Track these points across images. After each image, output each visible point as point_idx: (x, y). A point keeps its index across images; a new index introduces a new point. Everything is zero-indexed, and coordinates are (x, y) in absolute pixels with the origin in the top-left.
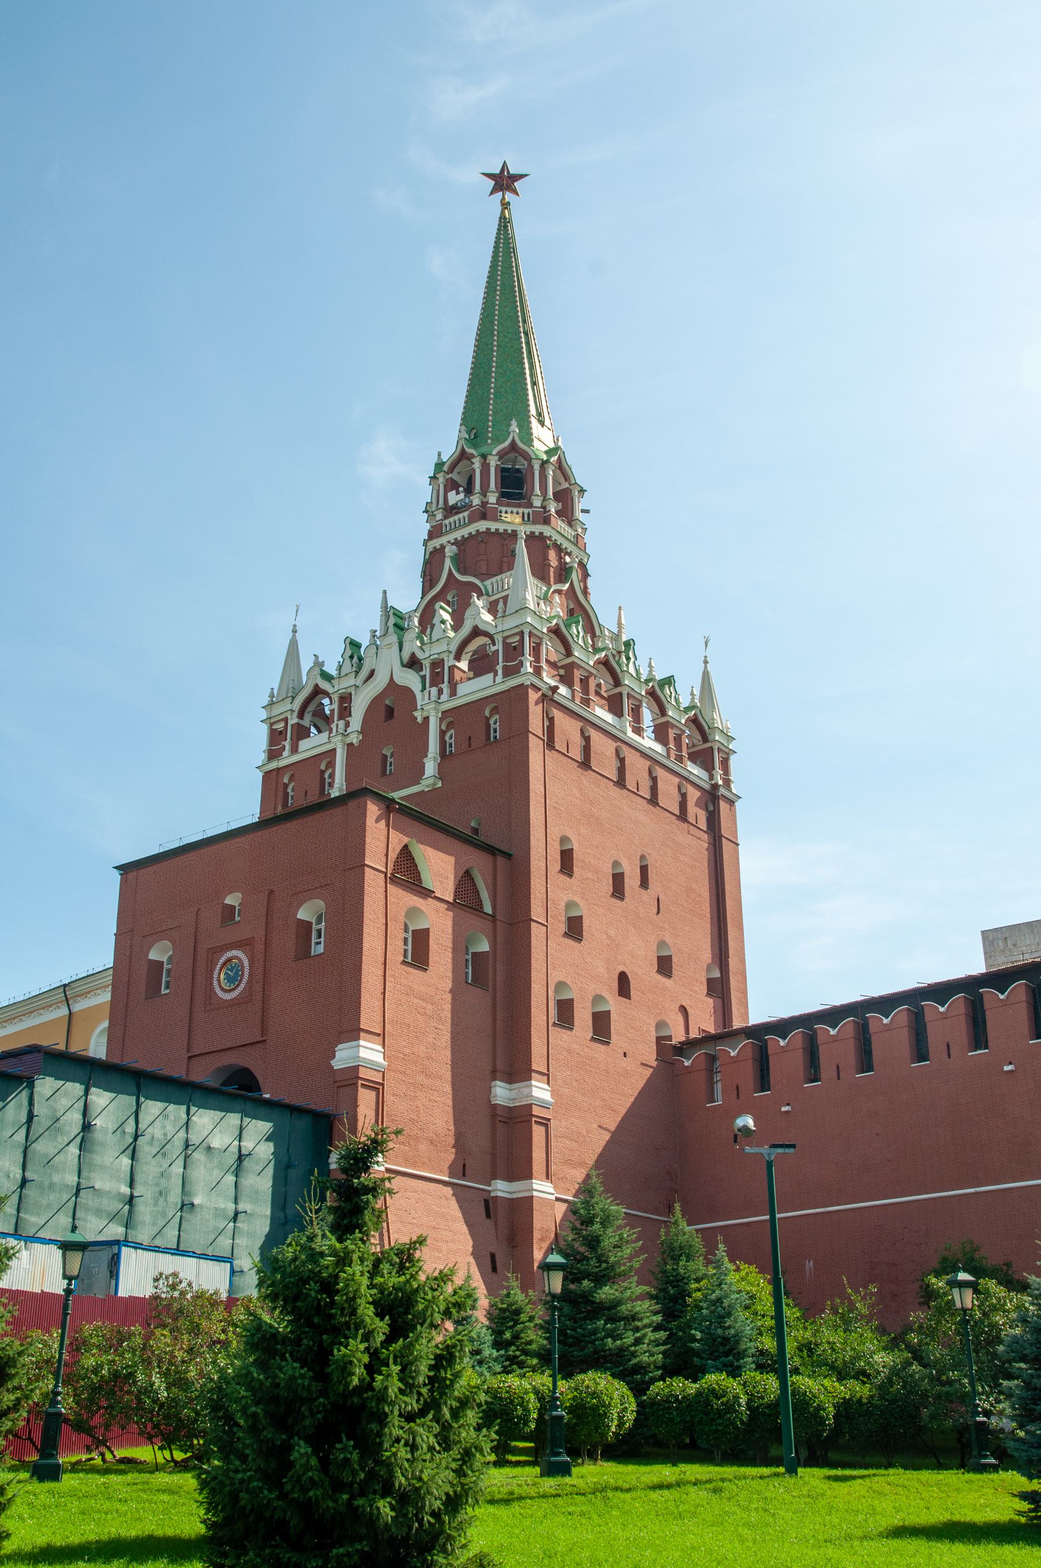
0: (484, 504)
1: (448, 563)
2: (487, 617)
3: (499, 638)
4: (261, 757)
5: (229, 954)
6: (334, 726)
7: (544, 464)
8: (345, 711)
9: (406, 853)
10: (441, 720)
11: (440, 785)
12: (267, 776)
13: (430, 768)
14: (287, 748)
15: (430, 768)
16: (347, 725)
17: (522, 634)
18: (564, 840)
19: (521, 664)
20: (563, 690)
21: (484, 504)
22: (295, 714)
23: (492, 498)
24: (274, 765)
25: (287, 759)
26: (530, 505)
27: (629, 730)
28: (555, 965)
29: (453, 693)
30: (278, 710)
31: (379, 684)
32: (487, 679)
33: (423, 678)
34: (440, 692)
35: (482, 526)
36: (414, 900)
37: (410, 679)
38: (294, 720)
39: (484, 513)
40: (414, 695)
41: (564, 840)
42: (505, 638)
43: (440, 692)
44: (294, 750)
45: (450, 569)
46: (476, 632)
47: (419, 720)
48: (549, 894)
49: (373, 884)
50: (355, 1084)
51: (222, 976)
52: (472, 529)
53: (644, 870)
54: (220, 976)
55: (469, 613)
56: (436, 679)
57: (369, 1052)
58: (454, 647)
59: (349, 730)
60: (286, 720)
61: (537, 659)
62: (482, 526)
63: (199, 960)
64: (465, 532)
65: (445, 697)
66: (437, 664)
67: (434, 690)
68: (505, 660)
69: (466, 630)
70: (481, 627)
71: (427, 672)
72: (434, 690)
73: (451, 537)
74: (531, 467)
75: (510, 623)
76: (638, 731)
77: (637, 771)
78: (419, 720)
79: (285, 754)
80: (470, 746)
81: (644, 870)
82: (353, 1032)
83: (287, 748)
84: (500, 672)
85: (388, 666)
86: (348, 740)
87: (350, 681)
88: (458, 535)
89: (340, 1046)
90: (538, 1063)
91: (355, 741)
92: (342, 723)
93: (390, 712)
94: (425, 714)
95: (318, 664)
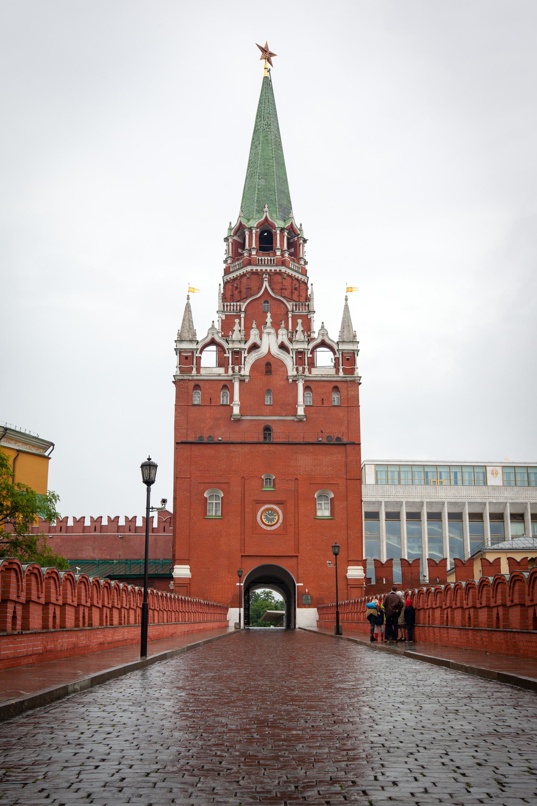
0: (282, 255)
1: (266, 284)
5: (268, 506)
6: (230, 366)
10: (303, 384)
11: (305, 420)
14: (194, 369)
16: (240, 369)
21: (282, 255)
22: (198, 352)
23: (286, 255)
26: (299, 263)
29: (310, 373)
30: (185, 346)
34: (304, 369)
35: (283, 269)
38: (198, 355)
39: (283, 263)
40: (284, 366)
43: (304, 369)
45: (266, 288)
47: (291, 380)
51: (263, 517)
52: (278, 269)
59: (242, 373)
62: (283, 269)
64: (273, 269)
65: (307, 373)
66: (300, 353)
70: (327, 341)
71: (293, 354)
72: (301, 368)
73: (264, 269)
78: (291, 380)
79: (194, 372)
80: (323, 404)
83: (194, 369)
84: (341, 370)
86: (242, 378)
87: (242, 346)
88: (268, 269)
89: (349, 567)
91: (247, 380)
92: (237, 368)
94: (295, 379)
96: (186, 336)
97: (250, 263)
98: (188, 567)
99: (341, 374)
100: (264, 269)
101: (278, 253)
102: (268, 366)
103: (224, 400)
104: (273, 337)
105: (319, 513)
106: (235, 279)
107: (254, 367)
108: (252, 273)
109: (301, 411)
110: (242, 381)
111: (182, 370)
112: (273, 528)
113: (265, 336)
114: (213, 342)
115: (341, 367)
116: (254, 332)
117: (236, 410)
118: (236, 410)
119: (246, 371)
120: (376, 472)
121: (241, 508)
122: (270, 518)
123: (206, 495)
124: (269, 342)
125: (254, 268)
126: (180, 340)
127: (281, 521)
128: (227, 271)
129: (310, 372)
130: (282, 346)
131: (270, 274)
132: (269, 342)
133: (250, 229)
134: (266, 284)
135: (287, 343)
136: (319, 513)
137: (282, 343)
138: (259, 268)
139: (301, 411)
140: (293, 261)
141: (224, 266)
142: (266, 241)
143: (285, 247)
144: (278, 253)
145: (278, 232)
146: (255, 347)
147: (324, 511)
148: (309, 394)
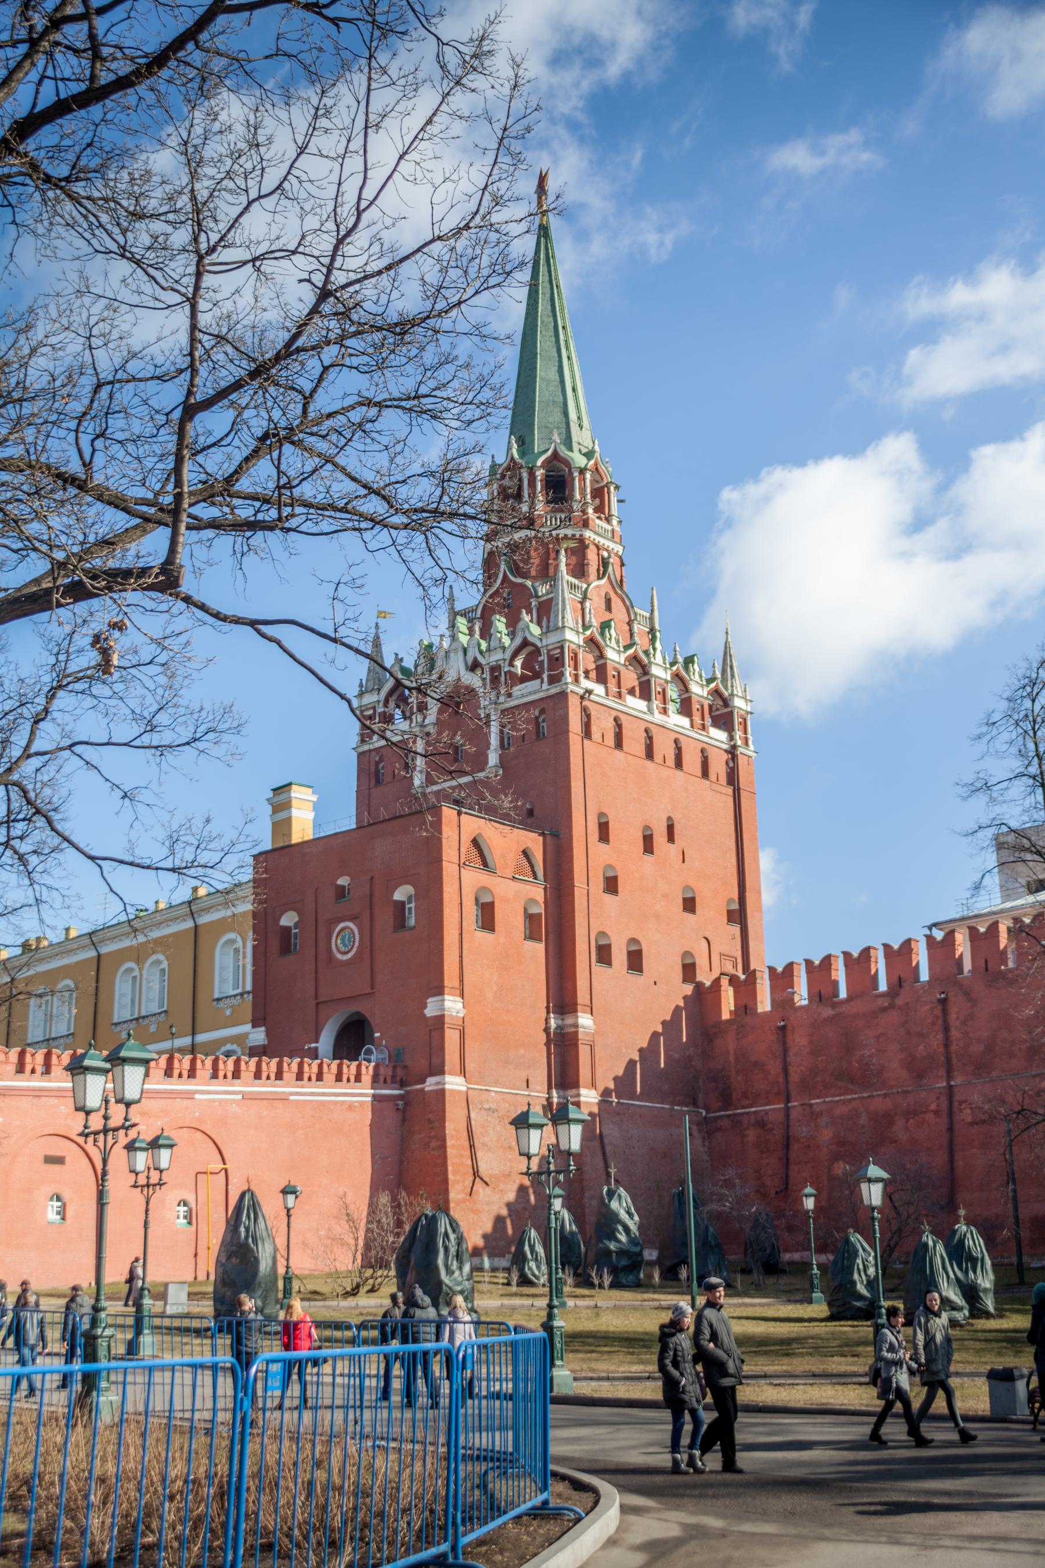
2: (535, 630)
3: (544, 651)
5: (342, 925)
7: (582, 471)
8: (422, 707)
9: (475, 843)
12: (361, 755)
13: (493, 758)
15: (493, 758)
17: (562, 648)
18: (601, 815)
19: (562, 674)
20: (599, 689)
24: (366, 748)
27: (656, 712)
28: (596, 915)
32: (534, 684)
33: (484, 679)
36: (482, 878)
37: (473, 680)
41: (601, 815)
42: (549, 651)
43: (498, 695)
46: (525, 643)
48: (589, 859)
49: (449, 869)
50: (443, 1028)
53: (670, 828)
54: (336, 942)
55: (521, 625)
56: (495, 680)
57: (452, 1005)
58: (508, 655)
59: (427, 722)
60: (374, 708)
61: (576, 668)
63: (319, 927)
65: (502, 699)
66: (495, 669)
67: (494, 693)
68: (549, 670)
69: (518, 641)
70: (530, 639)
71: (487, 675)
74: (571, 473)
75: (552, 639)
76: (665, 711)
77: (664, 748)
81: (670, 828)
82: (439, 990)
85: (456, 670)
86: (427, 730)
90: (582, 997)
95: (399, 660)
98: (263, 1029)
99: (545, 686)
112: (349, 956)
115: (545, 676)
127: (357, 944)
134: (503, 567)
137: (475, 659)
145: (525, 475)
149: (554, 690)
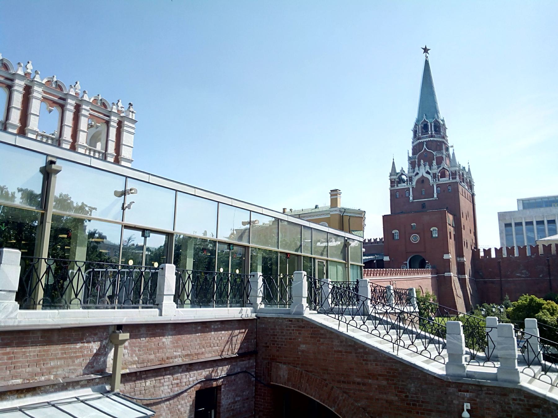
0: (432, 133)
1: (425, 146)
4: (389, 187)
21: (432, 133)
23: (433, 132)
24: (393, 189)
25: (396, 188)
30: (392, 177)
31: (420, 175)
35: (432, 139)
39: (432, 137)
40: (428, 179)
44: (397, 186)
52: (430, 139)
62: (432, 139)
64: (428, 139)
88: (426, 140)
93: (423, 181)
96: (393, 174)
97: (419, 139)
99: (451, 179)
100: (424, 140)
101: (430, 133)
102: (423, 180)
103: (407, 195)
104: (424, 170)
105: (434, 236)
106: (416, 146)
107: (417, 182)
108: (420, 143)
109: (435, 196)
110: (413, 188)
111: (391, 186)
113: (421, 169)
114: (402, 174)
116: (417, 168)
117: (411, 198)
118: (411, 198)
119: (414, 183)
120: (523, 204)
121: (405, 236)
122: (415, 239)
123: (393, 232)
124: (422, 171)
125: (420, 141)
126: (391, 175)
128: (413, 143)
129: (439, 180)
130: (428, 173)
131: (427, 142)
132: (422, 171)
133: (418, 125)
134: (425, 146)
135: (429, 171)
136: (434, 236)
138: (422, 140)
139: (435, 196)
140: (438, 134)
141: (412, 140)
142: (425, 127)
143: (433, 130)
144: (430, 133)
146: (417, 174)
147: (435, 235)
148: (439, 189)
149: (454, 181)
